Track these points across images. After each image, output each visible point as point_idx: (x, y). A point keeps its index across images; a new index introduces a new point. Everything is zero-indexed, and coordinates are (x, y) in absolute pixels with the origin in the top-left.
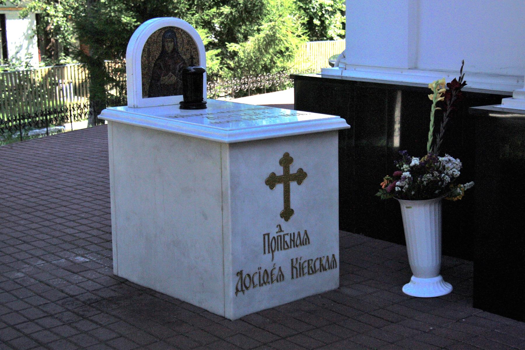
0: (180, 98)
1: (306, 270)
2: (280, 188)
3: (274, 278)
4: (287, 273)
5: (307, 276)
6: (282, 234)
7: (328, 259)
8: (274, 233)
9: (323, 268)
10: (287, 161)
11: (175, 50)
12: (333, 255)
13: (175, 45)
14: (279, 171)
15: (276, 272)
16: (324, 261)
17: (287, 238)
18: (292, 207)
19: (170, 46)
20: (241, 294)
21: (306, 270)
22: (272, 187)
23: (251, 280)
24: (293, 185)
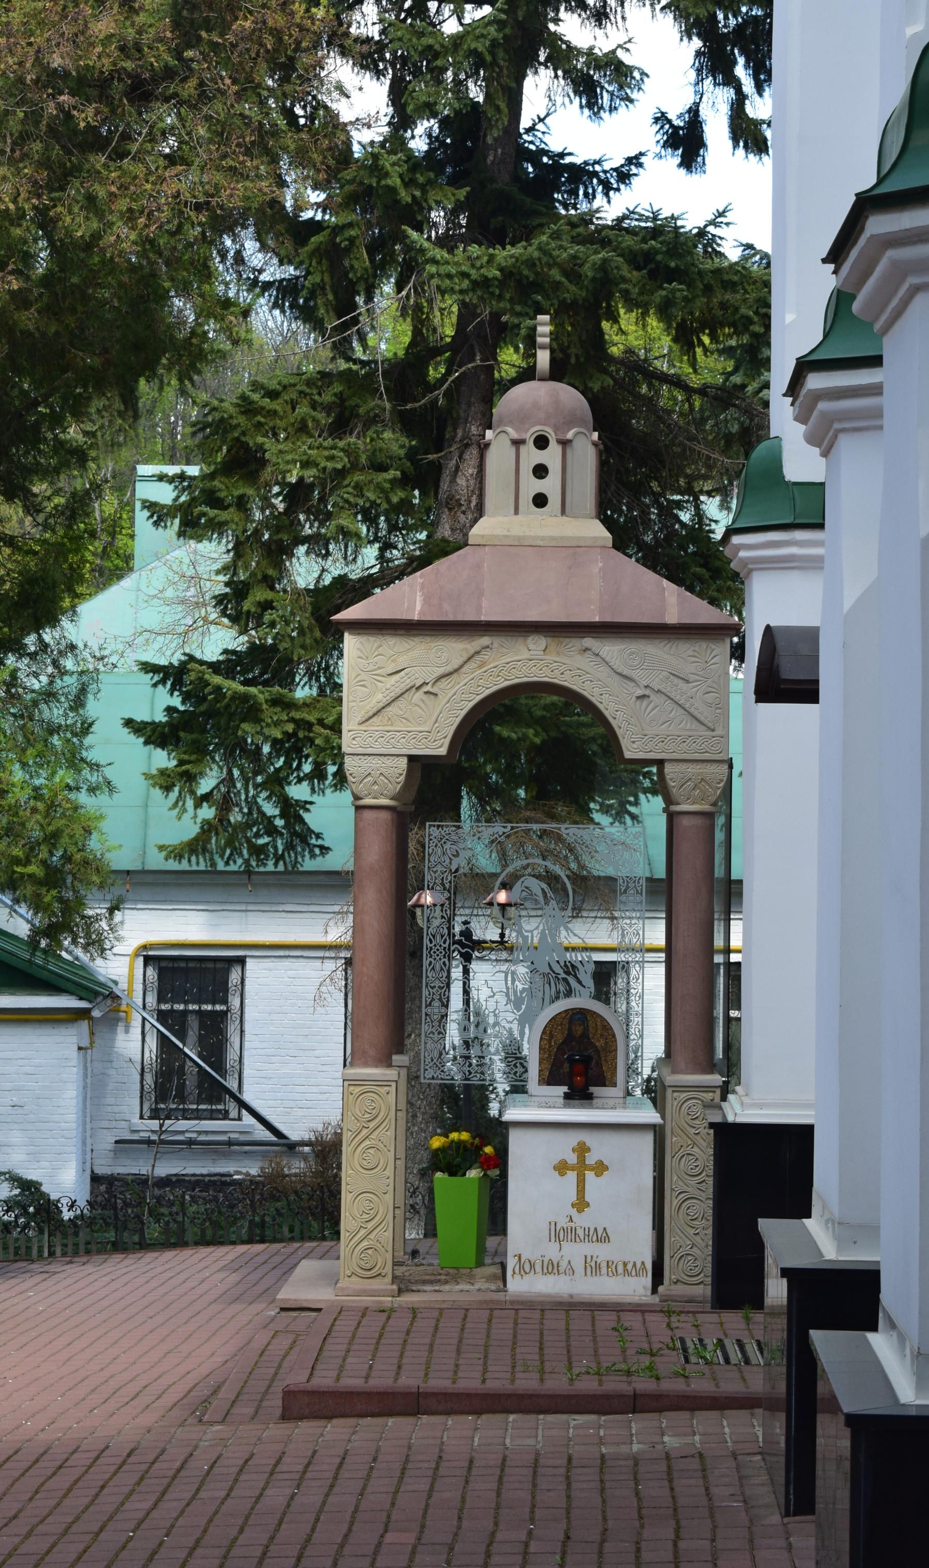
0: (565, 1089)
1: (604, 1270)
2: (572, 1176)
3: (561, 1270)
4: (579, 1266)
5: (605, 1278)
6: (572, 1225)
7: (635, 1265)
8: (563, 1222)
9: (626, 1272)
10: (582, 1150)
11: (585, 1035)
12: (643, 1263)
13: (586, 1029)
14: (572, 1159)
15: (564, 1264)
16: (629, 1267)
17: (580, 1232)
18: (588, 1198)
19: (579, 1030)
20: (517, 1277)
21: (604, 1270)
22: (562, 1174)
23: (532, 1266)
24: (590, 1175)
